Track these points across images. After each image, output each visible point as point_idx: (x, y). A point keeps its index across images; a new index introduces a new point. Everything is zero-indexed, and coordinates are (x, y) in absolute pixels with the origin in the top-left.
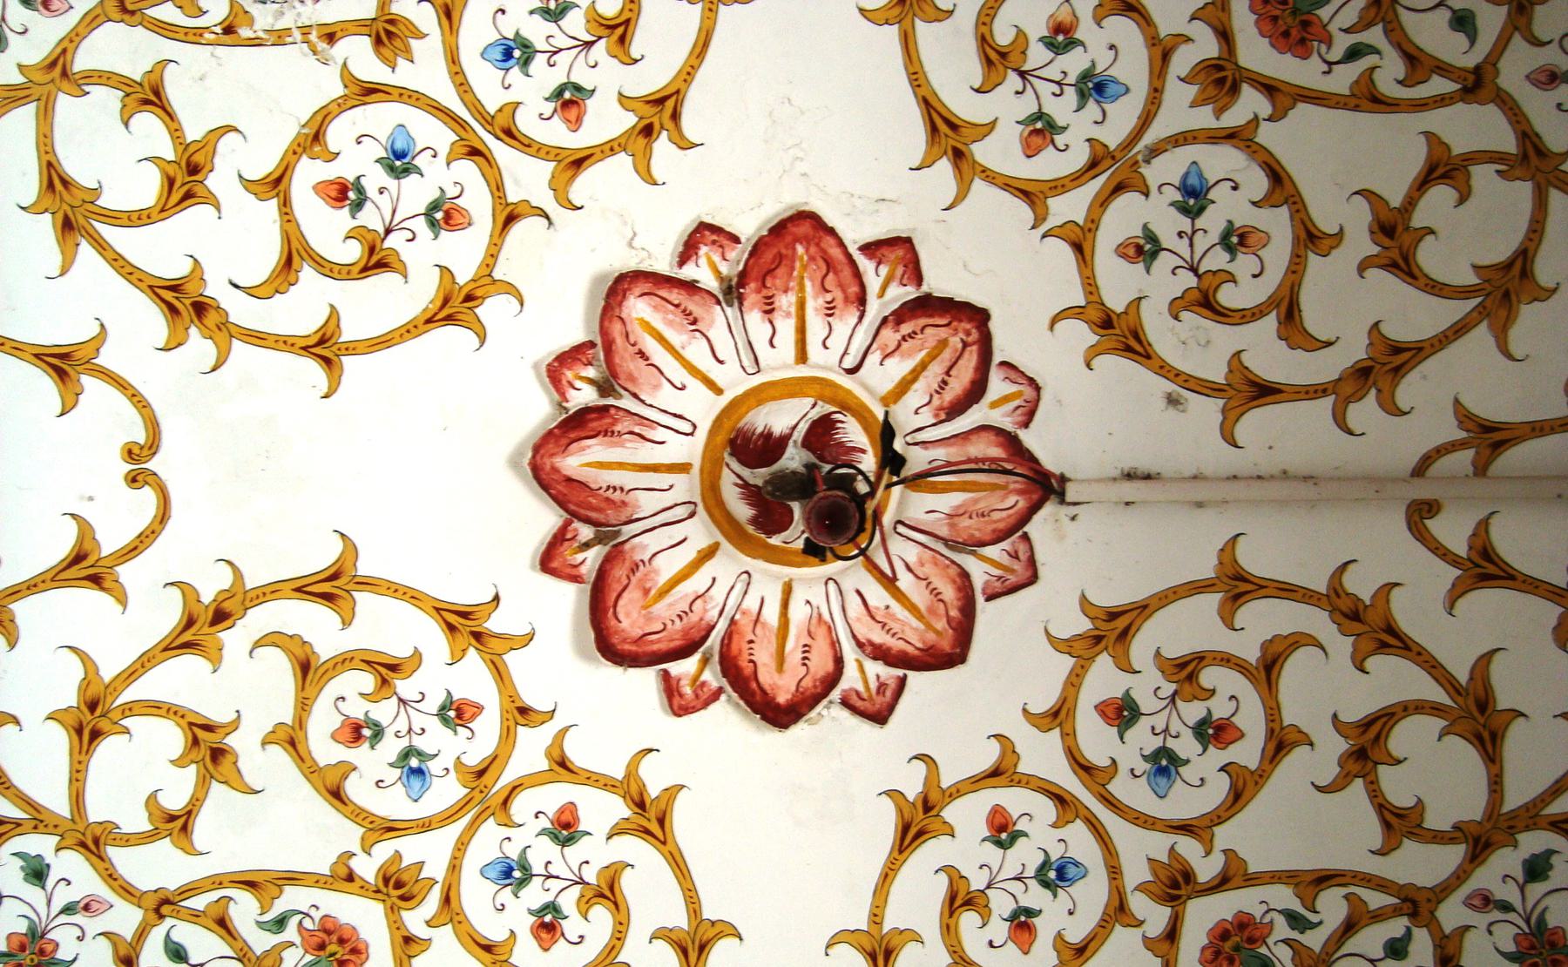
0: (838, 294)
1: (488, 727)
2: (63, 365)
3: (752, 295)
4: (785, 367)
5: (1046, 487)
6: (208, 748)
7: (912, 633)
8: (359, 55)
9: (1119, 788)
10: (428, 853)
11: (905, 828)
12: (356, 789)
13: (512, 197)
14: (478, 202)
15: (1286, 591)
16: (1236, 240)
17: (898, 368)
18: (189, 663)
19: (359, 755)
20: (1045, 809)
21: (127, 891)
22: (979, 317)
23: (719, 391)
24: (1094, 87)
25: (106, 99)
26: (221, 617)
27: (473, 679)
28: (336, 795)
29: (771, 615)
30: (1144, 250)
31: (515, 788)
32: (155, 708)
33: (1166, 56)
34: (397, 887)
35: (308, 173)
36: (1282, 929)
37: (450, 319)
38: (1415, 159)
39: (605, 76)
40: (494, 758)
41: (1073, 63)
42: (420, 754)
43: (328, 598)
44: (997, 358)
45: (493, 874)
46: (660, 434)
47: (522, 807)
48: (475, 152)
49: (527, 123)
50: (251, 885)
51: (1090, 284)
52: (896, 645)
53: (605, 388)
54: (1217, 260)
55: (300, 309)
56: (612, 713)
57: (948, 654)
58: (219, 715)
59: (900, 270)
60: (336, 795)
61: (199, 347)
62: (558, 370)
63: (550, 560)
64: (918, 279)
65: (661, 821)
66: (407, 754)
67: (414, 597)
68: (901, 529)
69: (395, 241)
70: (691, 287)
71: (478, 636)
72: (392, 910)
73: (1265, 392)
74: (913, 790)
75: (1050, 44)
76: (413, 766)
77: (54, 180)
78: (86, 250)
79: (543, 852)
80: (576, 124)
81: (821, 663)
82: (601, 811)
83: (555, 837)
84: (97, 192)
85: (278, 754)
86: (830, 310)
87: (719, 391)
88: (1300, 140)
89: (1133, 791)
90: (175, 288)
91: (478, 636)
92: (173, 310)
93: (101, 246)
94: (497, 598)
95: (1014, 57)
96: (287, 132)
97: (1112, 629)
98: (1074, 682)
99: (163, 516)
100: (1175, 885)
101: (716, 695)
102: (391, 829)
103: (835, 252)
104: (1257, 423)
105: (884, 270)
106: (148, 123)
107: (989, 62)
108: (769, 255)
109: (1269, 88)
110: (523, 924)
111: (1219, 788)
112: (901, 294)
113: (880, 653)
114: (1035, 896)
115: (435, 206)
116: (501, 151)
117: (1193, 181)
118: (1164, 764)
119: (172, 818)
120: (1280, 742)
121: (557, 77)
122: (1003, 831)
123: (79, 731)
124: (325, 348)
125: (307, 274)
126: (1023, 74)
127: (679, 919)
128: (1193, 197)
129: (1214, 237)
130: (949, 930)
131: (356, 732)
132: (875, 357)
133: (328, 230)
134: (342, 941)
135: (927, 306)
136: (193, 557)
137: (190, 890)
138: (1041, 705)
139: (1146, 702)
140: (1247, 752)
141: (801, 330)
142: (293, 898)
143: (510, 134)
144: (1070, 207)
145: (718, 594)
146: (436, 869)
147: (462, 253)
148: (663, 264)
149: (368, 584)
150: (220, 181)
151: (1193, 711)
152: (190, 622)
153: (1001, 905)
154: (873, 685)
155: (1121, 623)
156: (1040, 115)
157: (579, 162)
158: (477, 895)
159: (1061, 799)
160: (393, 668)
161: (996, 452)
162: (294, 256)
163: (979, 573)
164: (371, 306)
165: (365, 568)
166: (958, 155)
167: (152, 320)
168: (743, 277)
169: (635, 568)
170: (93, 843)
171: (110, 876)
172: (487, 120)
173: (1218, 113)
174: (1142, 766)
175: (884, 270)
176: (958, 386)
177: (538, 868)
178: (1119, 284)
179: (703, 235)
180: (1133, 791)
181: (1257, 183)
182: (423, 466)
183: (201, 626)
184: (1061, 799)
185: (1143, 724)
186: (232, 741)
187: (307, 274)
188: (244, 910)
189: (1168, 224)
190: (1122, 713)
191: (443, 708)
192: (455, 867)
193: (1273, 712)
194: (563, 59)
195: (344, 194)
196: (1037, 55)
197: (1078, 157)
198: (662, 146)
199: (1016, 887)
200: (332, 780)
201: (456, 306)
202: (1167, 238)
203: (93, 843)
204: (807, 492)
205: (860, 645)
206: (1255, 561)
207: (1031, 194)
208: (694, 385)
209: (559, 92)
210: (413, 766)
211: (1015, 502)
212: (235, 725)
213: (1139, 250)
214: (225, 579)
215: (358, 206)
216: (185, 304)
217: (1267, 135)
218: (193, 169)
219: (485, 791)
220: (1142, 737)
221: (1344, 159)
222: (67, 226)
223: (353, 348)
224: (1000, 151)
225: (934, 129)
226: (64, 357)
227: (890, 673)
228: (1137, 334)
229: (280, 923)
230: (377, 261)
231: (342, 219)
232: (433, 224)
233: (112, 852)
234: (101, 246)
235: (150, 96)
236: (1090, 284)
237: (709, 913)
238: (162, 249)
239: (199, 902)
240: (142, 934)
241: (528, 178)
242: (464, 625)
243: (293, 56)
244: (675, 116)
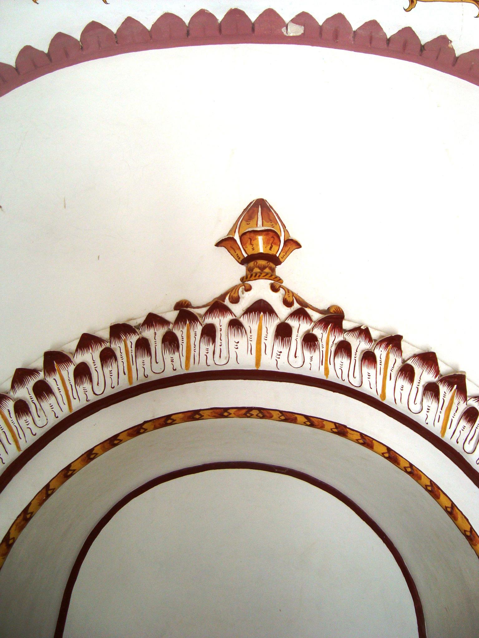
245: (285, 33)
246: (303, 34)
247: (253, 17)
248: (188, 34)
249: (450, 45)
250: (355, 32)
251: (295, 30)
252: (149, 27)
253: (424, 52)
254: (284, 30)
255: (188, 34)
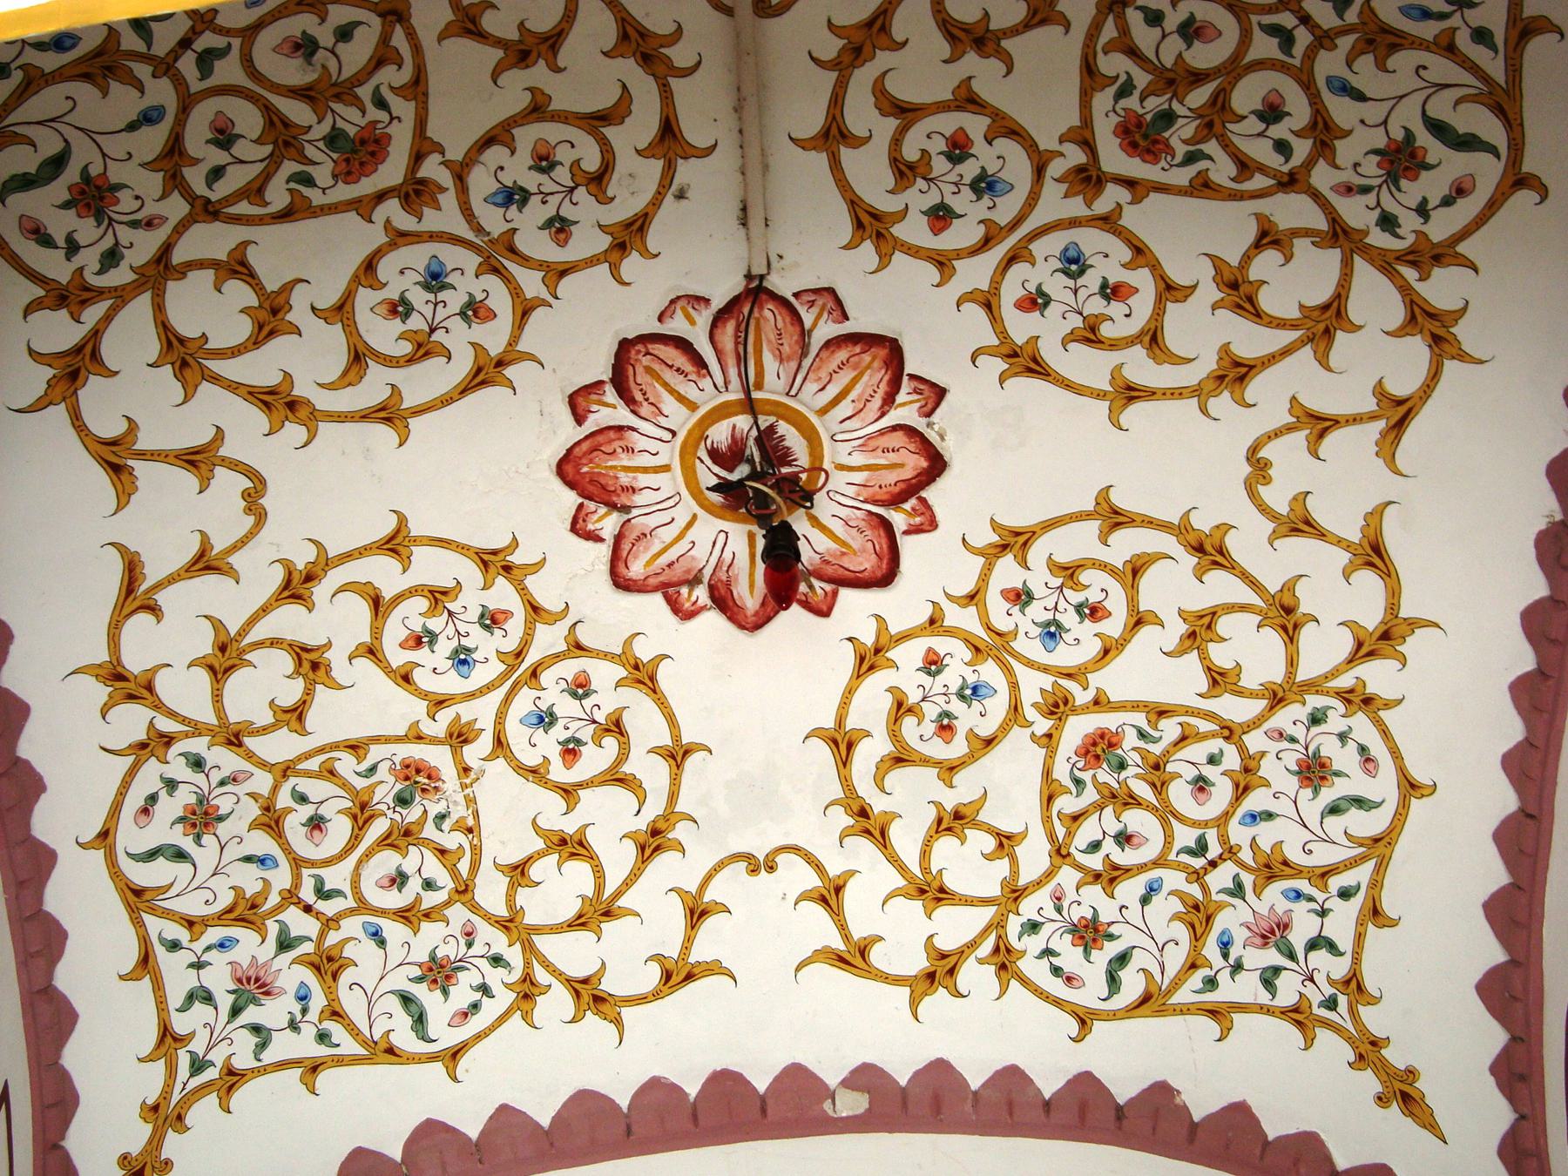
0: (616, 444)
1: (942, 645)
2: (697, 913)
3: (623, 500)
4: (674, 479)
5: (756, 292)
6: (953, 822)
7: (875, 378)
8: (474, 753)
9: (1003, 216)
10: (1033, 686)
11: (1030, 371)
12: (986, 729)
13: (563, 647)
14: (569, 668)
15: (837, 100)
16: (544, 162)
17: (669, 404)
18: (895, 832)
19: (962, 727)
20: (1019, 271)
21: (1049, 874)
22: (625, 346)
23: (695, 517)
24: (435, 280)
25: (523, 897)
26: (863, 813)
27: (909, 655)
28: (989, 742)
29: (859, 477)
30: (560, 228)
31: (989, 628)
32: (925, 854)
33: (403, 234)
34: (1058, 707)
35: (559, 773)
36: (1132, 102)
37: (652, 678)
38: (464, 46)
39: (471, 601)
40: (966, 641)
41: (418, 297)
42: (962, 688)
43: (850, 746)
44: (657, 328)
45: (1052, 644)
46: (727, 556)
47: (1002, 623)
48: (534, 674)
49: (511, 644)
50: (1050, 799)
51: (591, 262)
52: (883, 387)
53: (694, 581)
54: (563, 175)
55: (653, 774)
56: (933, 567)
57: (892, 352)
58: (932, 813)
59: (594, 397)
60: (989, 742)
61: (681, 832)
62: (684, 614)
63: (823, 611)
64: (600, 383)
65: (1018, 534)
66: (962, 697)
67: (849, 692)
68: (793, 392)
69: (600, 717)
70: (619, 539)
71: (877, 651)
72: (1075, 711)
73: (669, 130)
74: (1000, 365)
75: (406, 316)
76: (972, 693)
77: (579, 922)
78: (621, 902)
79: (1036, 611)
80: (508, 614)
81: (899, 439)
82: (1007, 573)
83: (1027, 604)
84: (583, 897)
85: (960, 778)
86: (629, 450)
87: (695, 517)
88: (455, 129)
89: (1005, 210)
90: (642, 848)
91: (877, 651)
92: (657, 849)
93: (619, 894)
94: (850, 639)
95: (420, 338)
96: (533, 788)
97: (871, 226)
98: (914, 251)
99: (795, 849)
100: (1088, 179)
101: (923, 501)
102: (1015, 708)
103: (585, 446)
104: (694, 131)
105: (594, 408)
106: (535, 872)
107: (427, 354)
108: (591, 488)
109: (418, 158)
110: (1089, 627)
111: (1004, 145)
112: (610, 395)
113: (889, 400)
114: (1091, 280)
115: (574, 695)
116: (532, 658)
117: (499, 199)
118: (984, 185)
119: (1001, 845)
120: (967, 100)
121: (476, 630)
122: (1036, 302)
123: (939, 900)
124: (677, 755)
125: (627, 768)
126: (432, 330)
127: (1093, 527)
128: (513, 197)
129: (544, 178)
130: (1114, 345)
131: (945, 728)
132: (663, 421)
133: (596, 758)
134: (1095, 744)
135: (620, 380)
136: (823, 831)
137: (1051, 836)
138: (933, 274)
139: (933, 198)
140: (976, 125)
141: (645, 470)
142: (1061, 772)
143: (519, 654)
144: (532, 284)
145: (843, 512)
146: (1047, 681)
147: (604, 675)
148: (603, 551)
149: (840, 721)
150: (570, 826)
151: (940, 165)
152: (868, 832)
153: (1096, 306)
154: (916, 397)
155: (866, 219)
156: (463, 314)
157: (535, 609)
158: (1065, 656)
159: (1011, 259)
160: (900, 705)
161: (730, 327)
162: (616, 777)
163: (827, 330)
164: (646, 726)
165: (829, 723)
166: (500, 363)
167: (665, 862)
168: (606, 504)
169: (828, 562)
170: (1015, 893)
171: (1039, 884)
172: (511, 669)
173: (443, 190)
174: (986, 201)
175: (594, 408)
176: (680, 360)
177: (1050, 616)
178: (587, 241)
179: (579, 527)
180: (1005, 210)
181: (496, 154)
182: (759, 699)
183: (869, 824)
184: (1011, 259)
185: (950, 200)
186: (949, 807)
187: (627, 768)
188: (1067, 804)
189: (537, 212)
190: (941, 217)
191: (929, 674)
192: (1045, 669)
193: (941, 107)
194: (462, 628)
195: (570, 751)
196: (416, 323)
197: (492, 282)
198: (517, 558)
199: (1082, 294)
200: (978, 745)
201: (643, 676)
202: (550, 210)
203: (1015, 893)
204: (762, 485)
205: (883, 415)
206: (812, 122)
207: (524, 311)
208: (690, 536)
209: (487, 628)
210: (972, 693)
211: (769, 314)
212: (938, 805)
213: (560, 231)
214: (838, 811)
215: (578, 742)
216: (653, 842)
217: (456, 153)
218: (563, 842)
219: (992, 646)
220: (962, 202)
221: (468, 94)
222: (607, 914)
223: (676, 737)
224: (494, 336)
225: (483, 383)
226: (692, 912)
227: (906, 385)
228: (628, 225)
229: (1078, 782)
230: (615, 726)
231: (588, 751)
232: (586, 695)
233: (1022, 882)
234: (619, 894)
235: (519, 872)
236: (591, 262)
237: (1090, 506)
238: (618, 858)
239: (1061, 832)
240: (1079, 867)
241: (549, 639)
242: (869, 660)
243: (481, 791)
244: (495, 553)
245: (830, 1112)
246: (869, 1111)
247: (761, 1085)
248: (629, 1131)
249: (1178, 1100)
250: (975, 1093)
251: (851, 1104)
252: (545, 1122)
253: (1125, 1122)
254: (827, 1105)
255: (629, 1131)
